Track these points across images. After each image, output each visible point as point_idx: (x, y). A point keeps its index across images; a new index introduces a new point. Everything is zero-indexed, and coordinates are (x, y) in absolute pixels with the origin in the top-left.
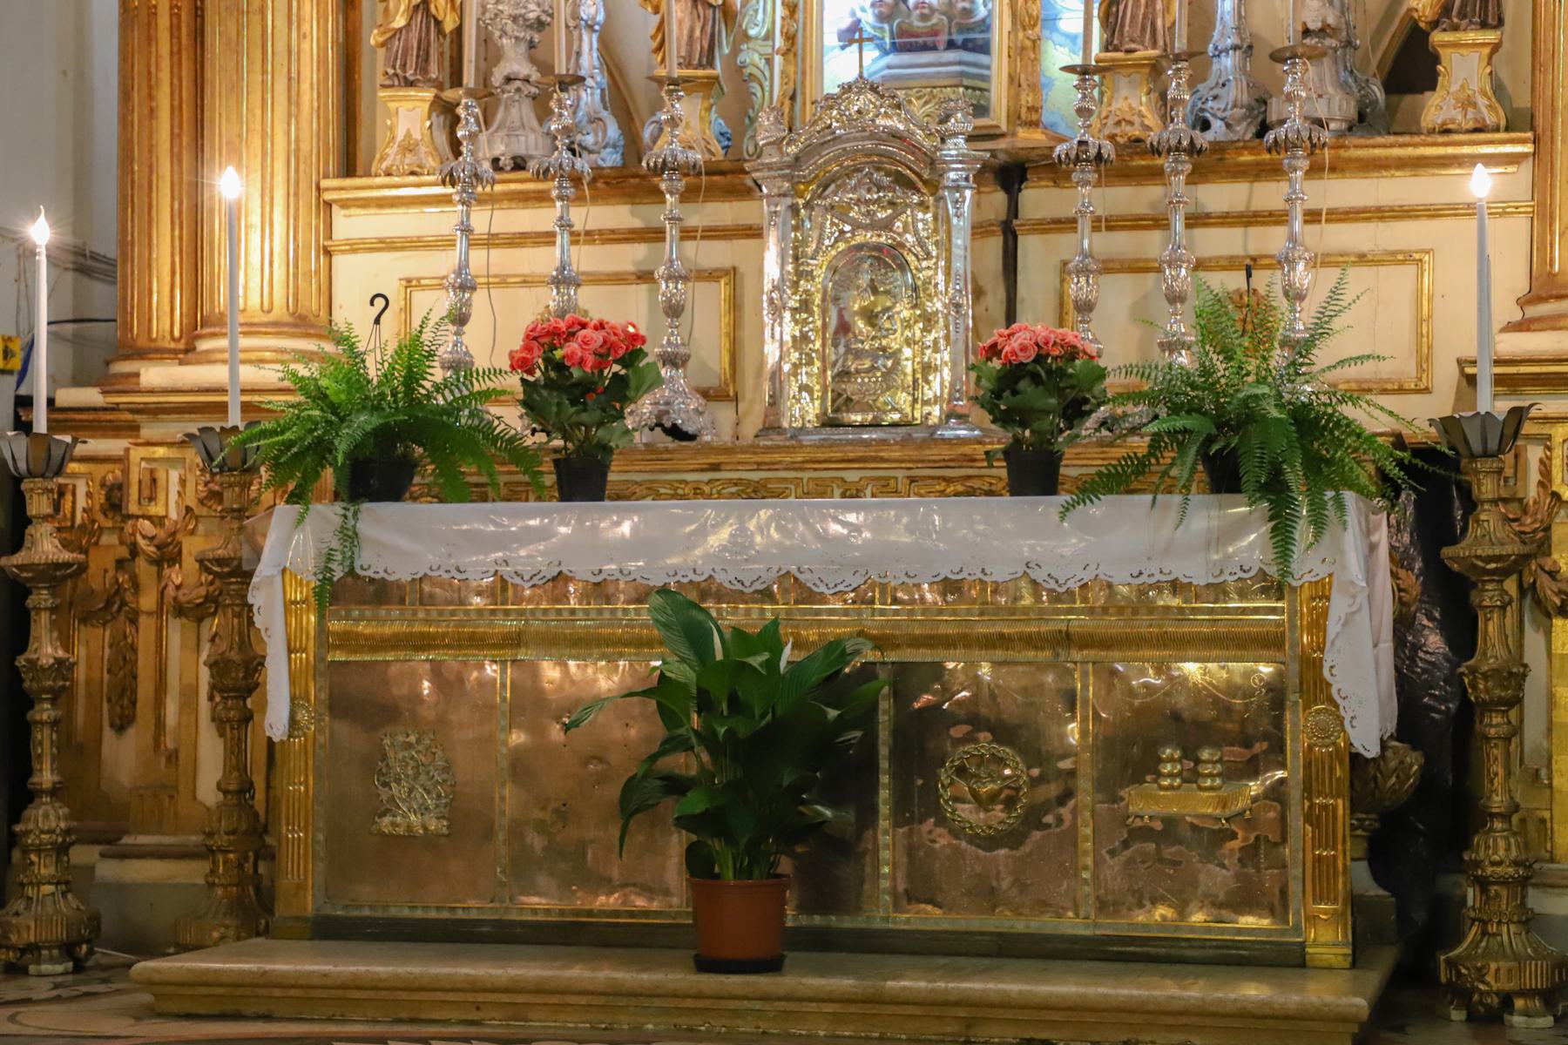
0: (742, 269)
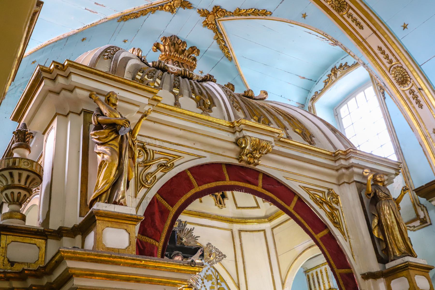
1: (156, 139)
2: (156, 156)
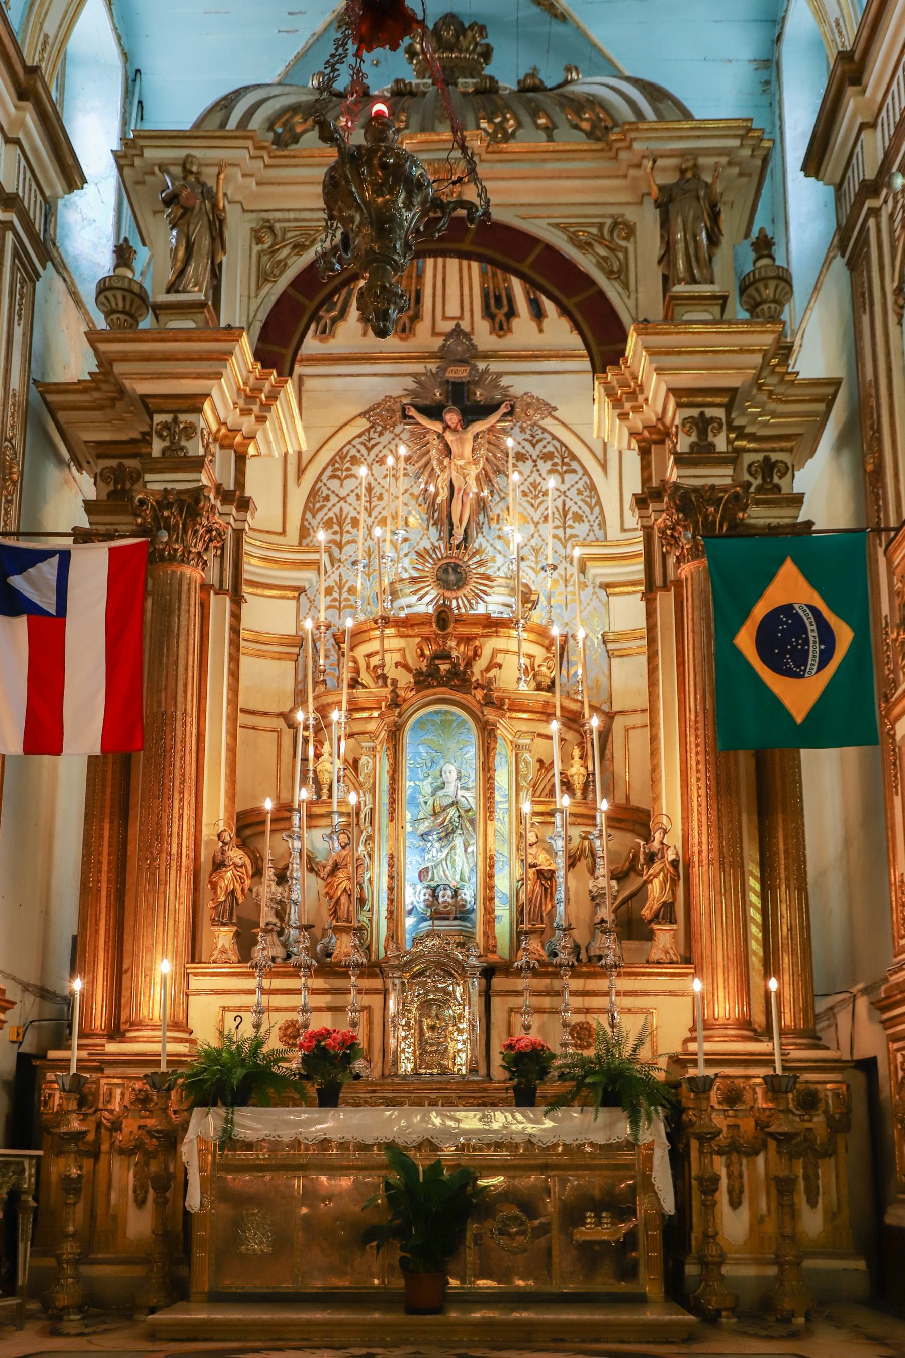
0: (373, 1007)
1: (289, 210)
2: (289, 235)
